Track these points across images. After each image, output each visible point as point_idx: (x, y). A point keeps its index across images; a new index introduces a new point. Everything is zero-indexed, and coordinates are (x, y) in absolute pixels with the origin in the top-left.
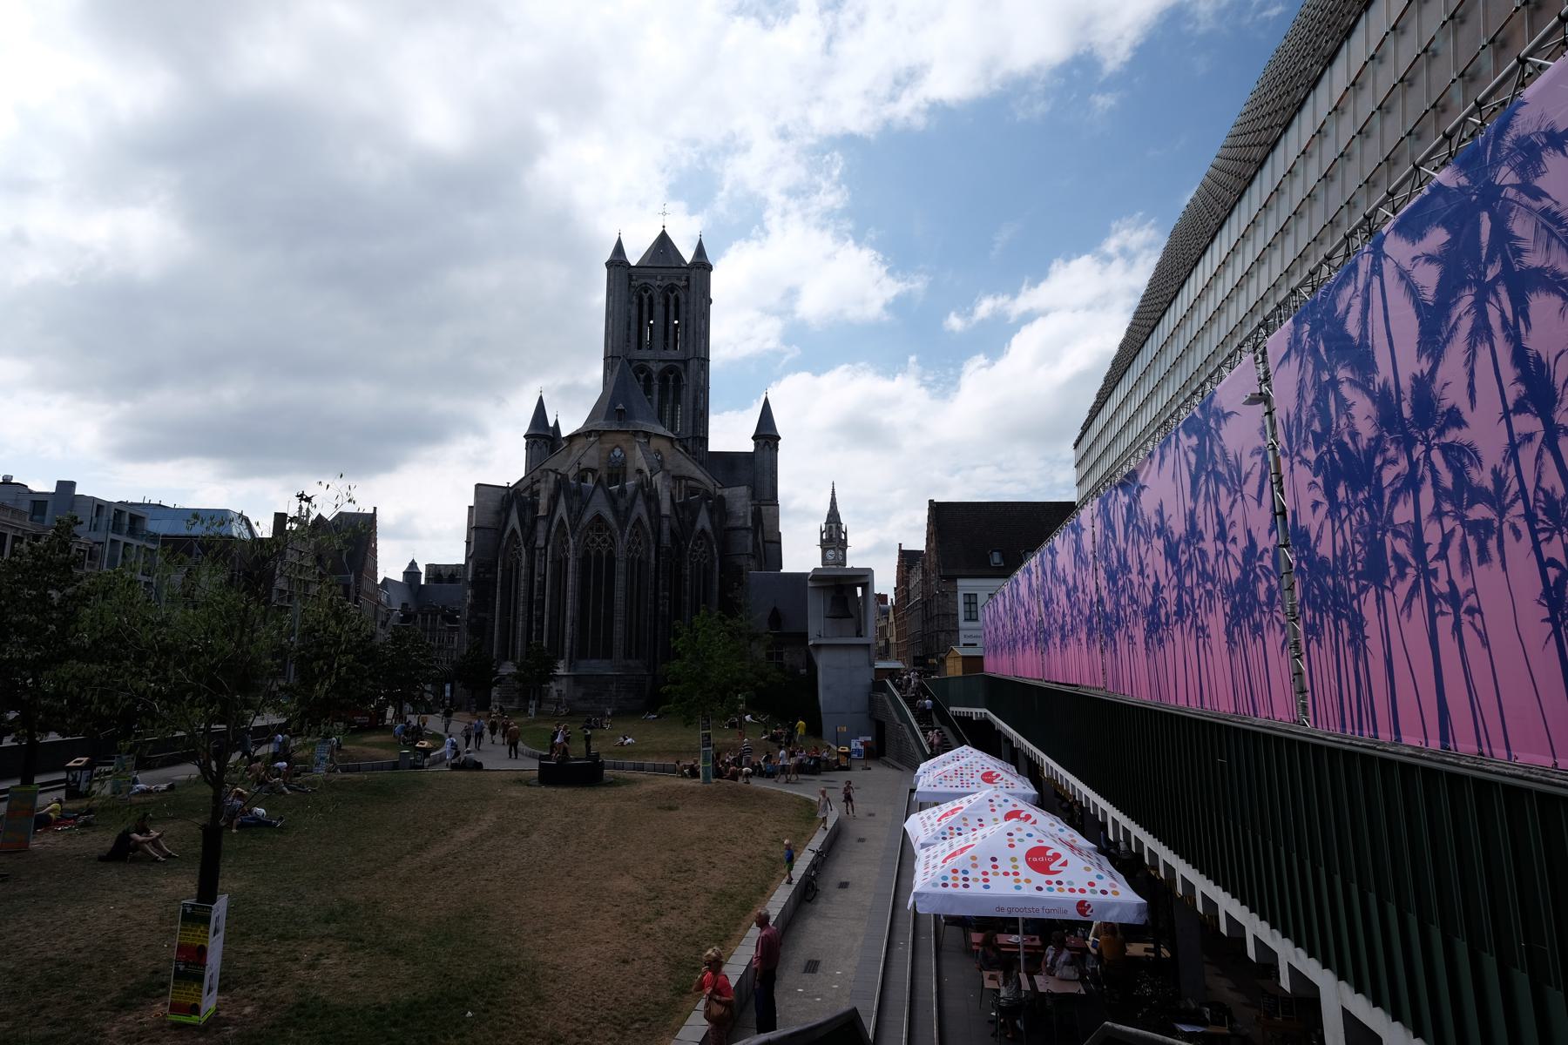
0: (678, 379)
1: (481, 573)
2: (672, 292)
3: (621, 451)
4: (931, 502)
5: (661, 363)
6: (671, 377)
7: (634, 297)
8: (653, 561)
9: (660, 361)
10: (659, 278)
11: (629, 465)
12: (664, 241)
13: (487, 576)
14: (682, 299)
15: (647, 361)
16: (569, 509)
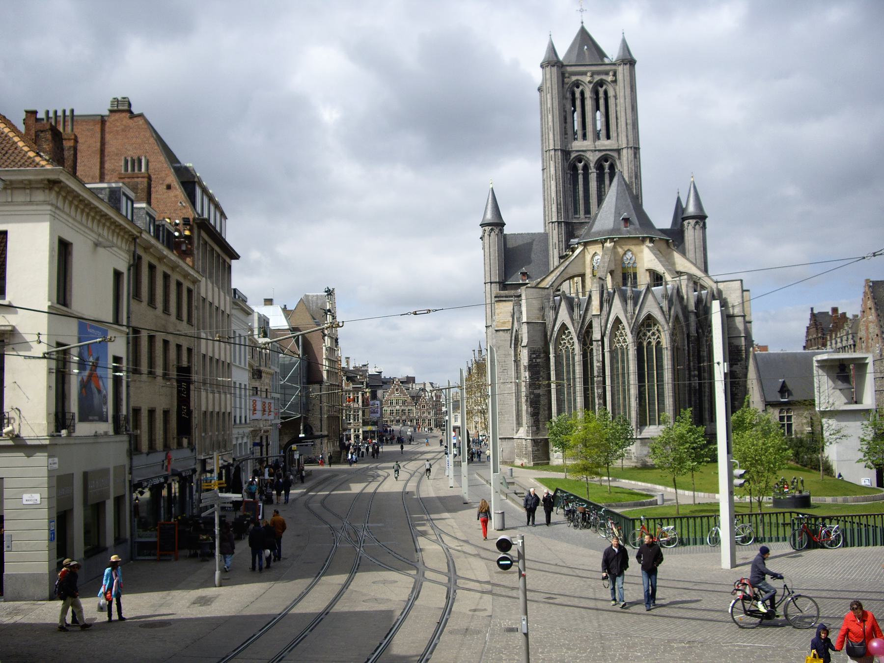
0: (612, 167)
1: (534, 358)
2: (602, 87)
3: (632, 254)
4: (867, 281)
5: (597, 152)
6: (607, 165)
7: (568, 93)
8: (686, 348)
9: (595, 151)
10: (589, 74)
11: (638, 265)
12: (584, 37)
13: (538, 360)
14: (611, 93)
15: (583, 151)
16: (626, 311)
